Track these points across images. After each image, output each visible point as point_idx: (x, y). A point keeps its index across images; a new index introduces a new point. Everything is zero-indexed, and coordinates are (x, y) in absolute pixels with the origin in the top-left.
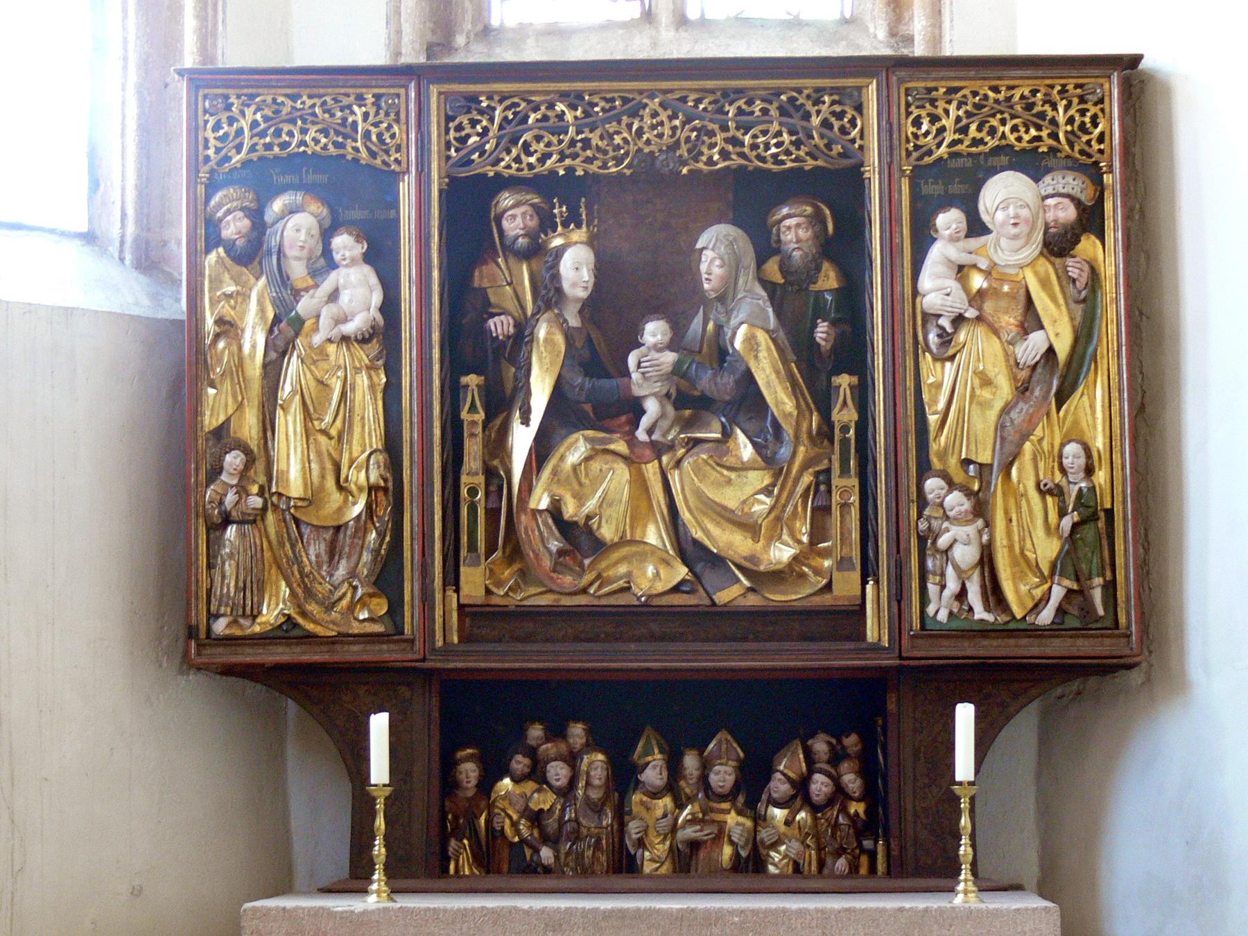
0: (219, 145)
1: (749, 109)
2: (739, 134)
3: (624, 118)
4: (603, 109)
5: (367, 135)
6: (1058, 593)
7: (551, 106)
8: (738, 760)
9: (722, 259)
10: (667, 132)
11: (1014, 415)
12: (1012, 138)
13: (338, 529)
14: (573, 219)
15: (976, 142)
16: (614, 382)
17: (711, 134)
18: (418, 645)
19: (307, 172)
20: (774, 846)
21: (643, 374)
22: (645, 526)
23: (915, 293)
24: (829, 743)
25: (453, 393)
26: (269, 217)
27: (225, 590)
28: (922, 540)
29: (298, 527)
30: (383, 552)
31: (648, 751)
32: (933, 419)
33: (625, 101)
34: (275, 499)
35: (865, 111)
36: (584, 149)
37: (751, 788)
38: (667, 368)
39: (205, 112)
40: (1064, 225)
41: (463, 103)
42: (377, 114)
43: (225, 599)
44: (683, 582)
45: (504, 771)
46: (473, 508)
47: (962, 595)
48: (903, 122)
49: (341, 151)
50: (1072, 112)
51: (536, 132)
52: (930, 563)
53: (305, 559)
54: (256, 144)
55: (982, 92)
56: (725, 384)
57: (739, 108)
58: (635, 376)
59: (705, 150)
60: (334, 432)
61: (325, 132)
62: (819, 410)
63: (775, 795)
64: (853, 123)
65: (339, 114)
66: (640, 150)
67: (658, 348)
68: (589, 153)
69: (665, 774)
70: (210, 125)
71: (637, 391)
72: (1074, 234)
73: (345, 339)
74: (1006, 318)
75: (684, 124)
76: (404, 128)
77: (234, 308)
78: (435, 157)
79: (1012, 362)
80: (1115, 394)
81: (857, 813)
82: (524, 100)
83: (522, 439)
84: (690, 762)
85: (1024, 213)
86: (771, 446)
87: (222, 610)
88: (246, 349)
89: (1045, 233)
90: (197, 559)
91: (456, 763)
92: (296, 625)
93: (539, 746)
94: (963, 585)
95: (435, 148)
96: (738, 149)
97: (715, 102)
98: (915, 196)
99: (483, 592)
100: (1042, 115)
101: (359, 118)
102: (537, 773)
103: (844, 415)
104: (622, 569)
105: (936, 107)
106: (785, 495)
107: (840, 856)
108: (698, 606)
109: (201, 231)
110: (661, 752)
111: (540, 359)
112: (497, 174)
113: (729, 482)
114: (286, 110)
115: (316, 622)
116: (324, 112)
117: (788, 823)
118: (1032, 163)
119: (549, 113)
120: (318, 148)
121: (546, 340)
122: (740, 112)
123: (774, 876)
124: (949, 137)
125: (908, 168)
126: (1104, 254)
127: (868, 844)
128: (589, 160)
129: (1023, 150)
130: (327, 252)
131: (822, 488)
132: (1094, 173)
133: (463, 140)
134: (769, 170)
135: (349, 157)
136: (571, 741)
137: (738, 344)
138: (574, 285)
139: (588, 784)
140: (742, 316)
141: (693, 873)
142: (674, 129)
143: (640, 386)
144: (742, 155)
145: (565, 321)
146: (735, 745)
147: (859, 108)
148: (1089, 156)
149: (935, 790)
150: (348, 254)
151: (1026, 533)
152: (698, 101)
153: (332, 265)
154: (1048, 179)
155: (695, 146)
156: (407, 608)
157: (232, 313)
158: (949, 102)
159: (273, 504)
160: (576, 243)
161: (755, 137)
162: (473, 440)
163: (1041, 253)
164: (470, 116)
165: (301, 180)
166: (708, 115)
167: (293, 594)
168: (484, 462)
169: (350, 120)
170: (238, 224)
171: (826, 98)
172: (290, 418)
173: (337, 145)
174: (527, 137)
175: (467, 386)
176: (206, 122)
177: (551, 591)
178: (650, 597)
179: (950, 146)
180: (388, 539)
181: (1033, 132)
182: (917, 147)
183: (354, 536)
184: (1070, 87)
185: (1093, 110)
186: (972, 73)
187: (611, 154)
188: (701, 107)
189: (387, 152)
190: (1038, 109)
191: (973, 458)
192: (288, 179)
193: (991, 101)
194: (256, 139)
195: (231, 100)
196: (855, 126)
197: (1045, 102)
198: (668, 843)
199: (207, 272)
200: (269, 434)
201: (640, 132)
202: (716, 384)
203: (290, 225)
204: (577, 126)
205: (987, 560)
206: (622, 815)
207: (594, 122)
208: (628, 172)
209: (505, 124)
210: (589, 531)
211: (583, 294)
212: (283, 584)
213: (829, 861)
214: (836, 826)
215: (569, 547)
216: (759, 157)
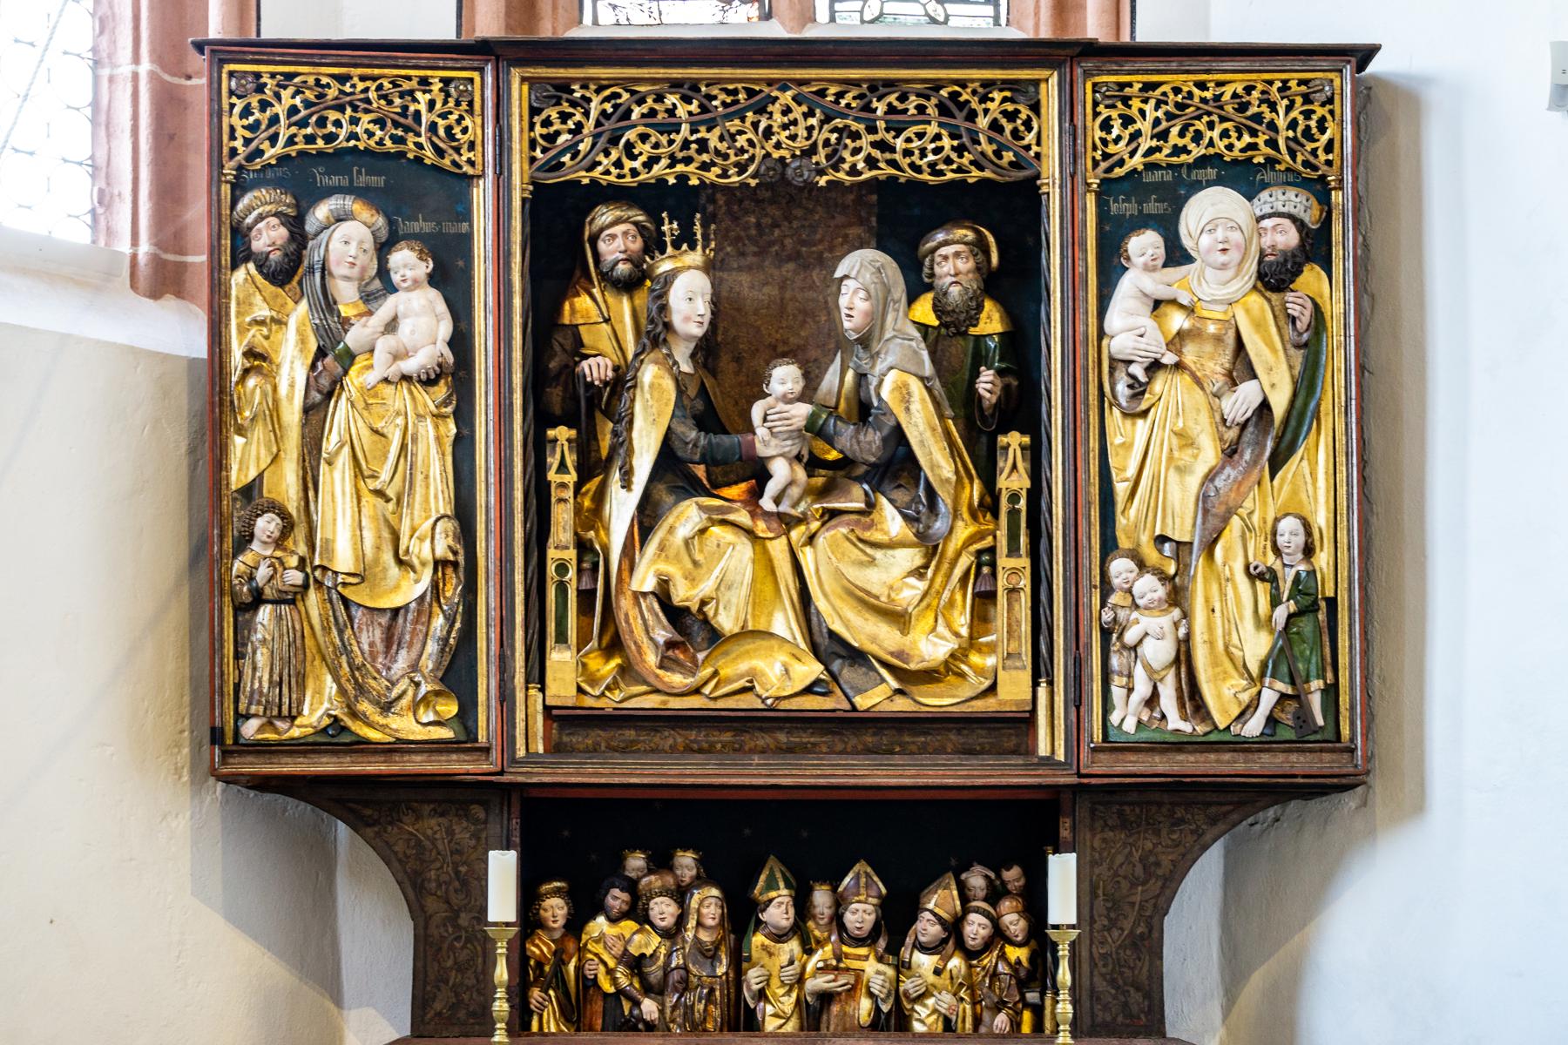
0: (248, 135)
2: (889, 137)
4: (724, 104)
5: (433, 127)
6: (1268, 699)
7: (660, 98)
8: (880, 896)
9: (867, 291)
10: (802, 133)
11: (1219, 482)
12: (1221, 145)
13: (396, 612)
14: (686, 239)
15: (1178, 150)
16: (736, 438)
17: (856, 136)
18: (495, 754)
19: (359, 172)
20: (920, 998)
22: (770, 614)
23: (1101, 334)
24: (987, 877)
25: (538, 447)
26: (310, 226)
27: (256, 685)
28: (1106, 634)
29: (347, 608)
30: (452, 641)
31: (771, 885)
32: (1121, 489)
33: (751, 93)
34: (318, 573)
35: (1043, 111)
36: (699, 152)
37: (893, 927)
38: (799, 422)
39: (231, 93)
40: (1284, 253)
41: (553, 92)
42: (445, 102)
43: (256, 697)
44: (817, 682)
45: (598, 908)
46: (562, 588)
47: (1152, 701)
48: (1089, 124)
49: (402, 147)
50: (1294, 114)
51: (641, 129)
52: (1115, 662)
53: (355, 648)
54: (295, 135)
55: (1185, 89)
56: (869, 443)
57: (890, 105)
58: (761, 432)
59: (846, 154)
60: (391, 493)
61: (380, 122)
62: (980, 477)
63: (922, 939)
64: (1028, 125)
65: (398, 101)
66: (768, 155)
67: (787, 400)
68: (705, 157)
69: (792, 911)
70: (237, 110)
71: (762, 451)
72: (1295, 263)
73: (406, 378)
74: (1211, 364)
75: (822, 123)
76: (478, 120)
77: (267, 338)
78: (516, 157)
79: (1218, 418)
80: (1341, 459)
81: (1019, 962)
83: (622, 506)
84: (821, 898)
85: (1236, 236)
86: (923, 518)
87: (253, 709)
88: (283, 390)
89: (1260, 262)
90: (222, 647)
91: (539, 898)
92: (345, 729)
93: (639, 879)
94: (1155, 687)
95: (516, 146)
96: (888, 156)
98: (1103, 215)
99: (574, 691)
100: (1258, 118)
101: (423, 108)
102: (638, 912)
103: (1012, 480)
105: (1130, 107)
106: (939, 580)
107: (1000, 1011)
108: (833, 711)
109: (227, 242)
110: (788, 886)
111: (645, 408)
112: (594, 181)
113: (873, 561)
114: (332, 93)
115: (370, 725)
116: (380, 97)
117: (937, 972)
118: (1244, 176)
119: (657, 107)
120: (372, 143)
121: (652, 386)
122: (891, 109)
123: (922, 1035)
124: (1146, 143)
125: (1094, 182)
127: (1032, 997)
128: (705, 167)
129: (1235, 161)
130: (383, 272)
131: (985, 570)
132: (1320, 189)
133: (551, 138)
134: (925, 183)
135: (411, 156)
136: (679, 872)
137: (885, 393)
138: (687, 319)
139: (699, 924)
140: (890, 360)
141: (824, 1031)
142: (810, 129)
143: (766, 444)
144: (893, 163)
145: (675, 363)
146: (876, 879)
147: (1036, 108)
148: (1315, 168)
149: (1116, 933)
150: (409, 274)
151: (1231, 624)
152: (840, 95)
153: (391, 288)
154: (1264, 195)
155: (835, 151)
156: (481, 710)
157: (266, 343)
158: (1145, 101)
159: (316, 580)
160: (689, 268)
161: (909, 140)
162: (562, 505)
163: (1255, 287)
164: (559, 108)
165: (351, 181)
166: (853, 113)
167: (342, 691)
168: (576, 534)
169: (412, 108)
170: (273, 234)
172: (337, 475)
173: (396, 140)
174: (631, 135)
175: (555, 440)
176: (232, 106)
177: (657, 691)
178: (777, 698)
179: (1145, 155)
180: (458, 625)
181: (1247, 139)
182: (1106, 156)
183: (416, 621)
184: (1293, 84)
185: (1321, 111)
186: (1174, 66)
187: (733, 159)
189: (457, 150)
190: (1253, 110)
191: (1169, 534)
192: (335, 180)
193: (1197, 100)
194: (294, 129)
195: (263, 80)
196: (1029, 129)
197: (1262, 102)
198: (794, 995)
199: (234, 292)
200: (311, 494)
201: (768, 133)
202: (859, 442)
203: (337, 235)
204: (692, 124)
205: (1183, 658)
206: (739, 961)
207: (714, 119)
208: (753, 183)
210: (706, 621)
211: (698, 331)
212: (329, 678)
213: (986, 1016)
214: (995, 975)
215: (679, 638)
216: (913, 166)
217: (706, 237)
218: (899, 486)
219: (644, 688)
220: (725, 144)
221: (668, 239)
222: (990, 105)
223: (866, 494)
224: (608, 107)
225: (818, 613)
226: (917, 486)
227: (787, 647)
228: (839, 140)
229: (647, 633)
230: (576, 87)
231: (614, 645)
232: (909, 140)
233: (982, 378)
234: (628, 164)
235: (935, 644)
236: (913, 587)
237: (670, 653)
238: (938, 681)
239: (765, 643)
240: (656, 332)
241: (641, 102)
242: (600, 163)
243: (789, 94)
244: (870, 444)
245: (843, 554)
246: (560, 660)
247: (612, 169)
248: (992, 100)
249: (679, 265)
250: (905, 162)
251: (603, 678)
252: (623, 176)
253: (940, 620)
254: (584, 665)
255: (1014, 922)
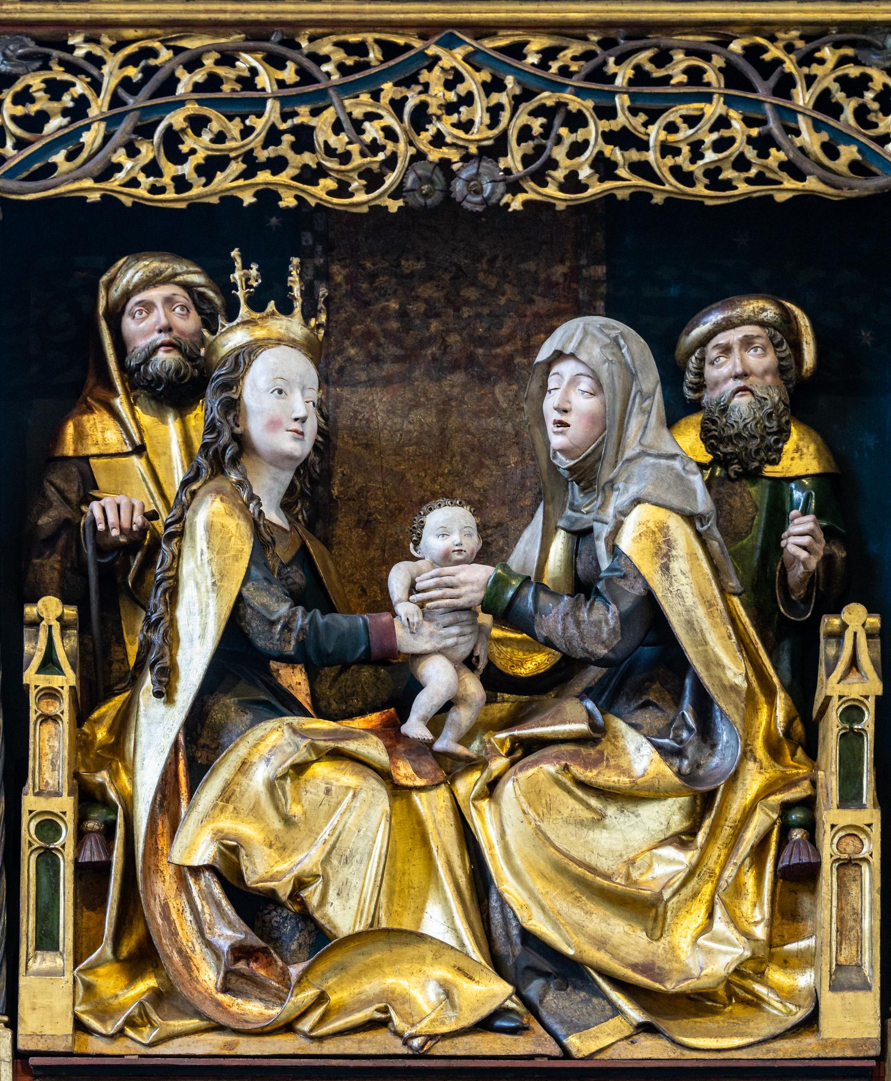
1: (658, 73)
3: (388, 86)
4: (342, 68)
7: (227, 59)
10: (479, 113)
14: (271, 295)
17: (576, 121)
21: (421, 604)
22: (421, 909)
33: (389, 50)
44: (501, 1012)
51: (192, 108)
56: (597, 624)
57: (638, 68)
58: (405, 609)
59: (559, 153)
66: (420, 156)
67: (446, 559)
71: (407, 642)
75: (517, 101)
82: (168, 48)
83: (157, 728)
86: (690, 751)
96: (634, 155)
97: (587, 56)
104: (371, 986)
106: (716, 852)
108: (531, 1057)
112: (108, 200)
113: (599, 820)
119: (222, 71)
122: (640, 77)
128: (309, 175)
134: (697, 206)
138: (274, 425)
144: (642, 169)
145: (252, 497)
155: (540, 150)
160: (279, 342)
164: (48, 75)
166: (574, 82)
168: (75, 775)
171: (827, 52)
174: (177, 119)
175: (35, 624)
177: (219, 1028)
178: (432, 1037)
187: (357, 161)
188: (555, 66)
202: (578, 624)
207: (323, 94)
208: (394, 206)
209: (122, 93)
210: (305, 916)
211: (300, 449)
216: (676, 171)
217: (309, 293)
218: (646, 705)
219: (194, 1023)
220: (344, 137)
221: (241, 294)
222: (815, 69)
223: (590, 714)
224: (133, 72)
225: (503, 902)
226: (677, 702)
227: (449, 956)
228: (547, 129)
229: (200, 934)
230: (75, 40)
232: (671, 128)
233: (793, 529)
234: (170, 170)
235: (709, 952)
236: (671, 861)
237: (241, 965)
238: (713, 1012)
239: (410, 951)
241: (193, 64)
242: (119, 167)
243: (459, 52)
244: (600, 625)
245: (549, 808)
247: (141, 177)
248: (822, 62)
249: (260, 333)
250: (662, 165)
251: (123, 1008)
252: (162, 190)
253: (719, 912)
254: (89, 988)
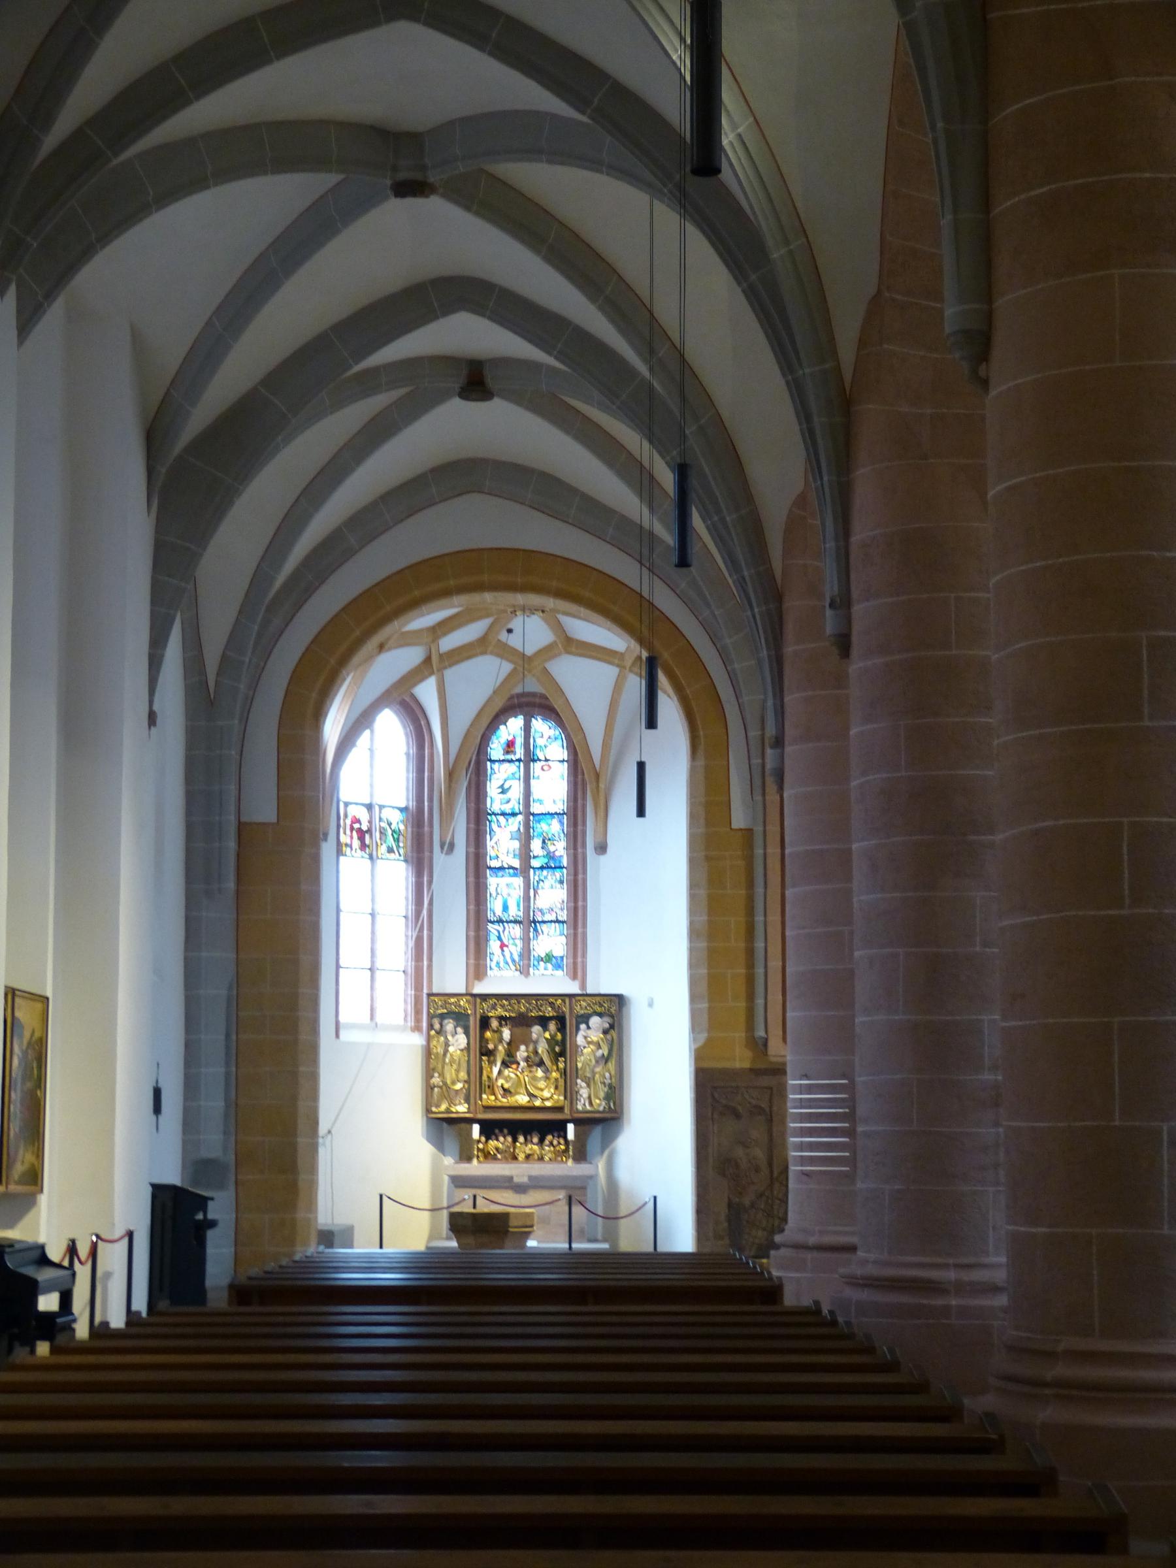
83: (496, 1070)
103: (561, 1065)
118: (600, 1015)
126: (614, 1033)
205: (589, 1098)
229: (499, 1092)
231: (494, 1094)
240: (501, 1040)
244: (537, 1060)
246: (484, 1096)
255: (562, 1141)
